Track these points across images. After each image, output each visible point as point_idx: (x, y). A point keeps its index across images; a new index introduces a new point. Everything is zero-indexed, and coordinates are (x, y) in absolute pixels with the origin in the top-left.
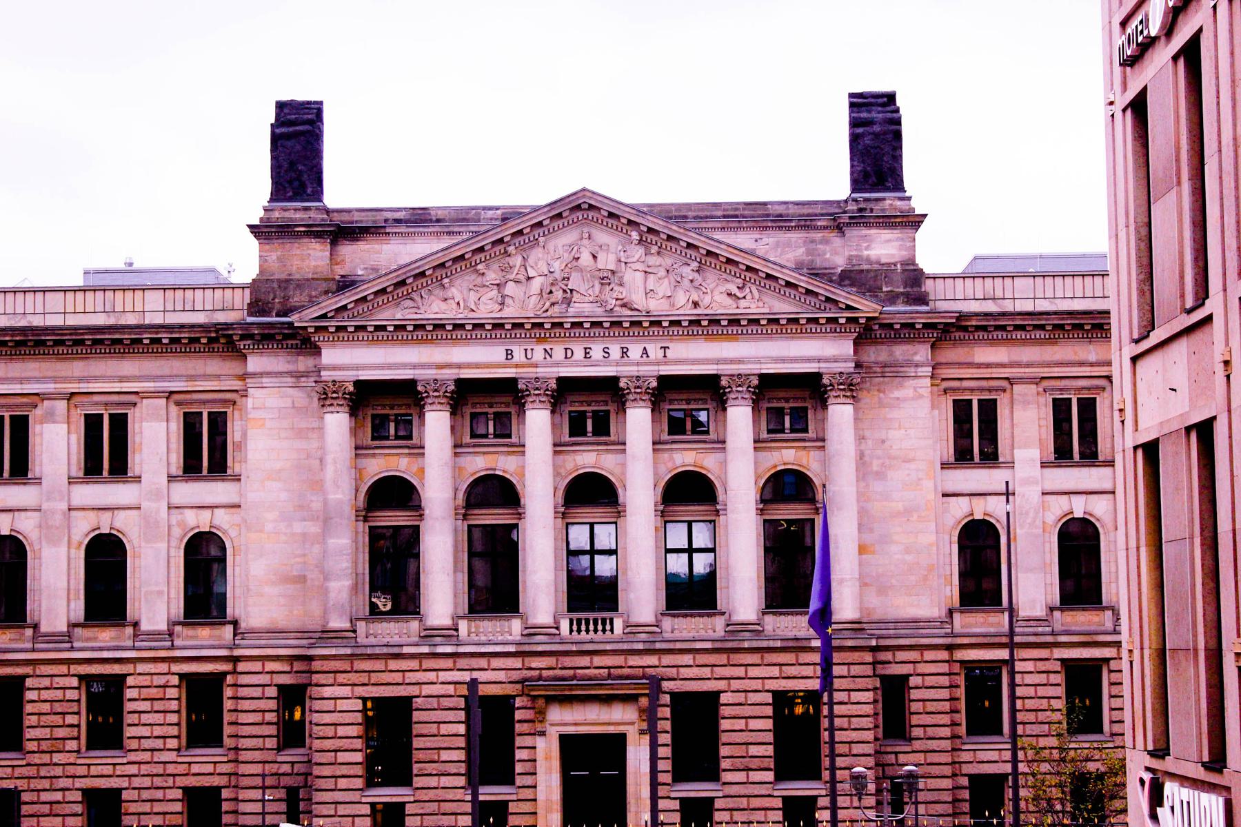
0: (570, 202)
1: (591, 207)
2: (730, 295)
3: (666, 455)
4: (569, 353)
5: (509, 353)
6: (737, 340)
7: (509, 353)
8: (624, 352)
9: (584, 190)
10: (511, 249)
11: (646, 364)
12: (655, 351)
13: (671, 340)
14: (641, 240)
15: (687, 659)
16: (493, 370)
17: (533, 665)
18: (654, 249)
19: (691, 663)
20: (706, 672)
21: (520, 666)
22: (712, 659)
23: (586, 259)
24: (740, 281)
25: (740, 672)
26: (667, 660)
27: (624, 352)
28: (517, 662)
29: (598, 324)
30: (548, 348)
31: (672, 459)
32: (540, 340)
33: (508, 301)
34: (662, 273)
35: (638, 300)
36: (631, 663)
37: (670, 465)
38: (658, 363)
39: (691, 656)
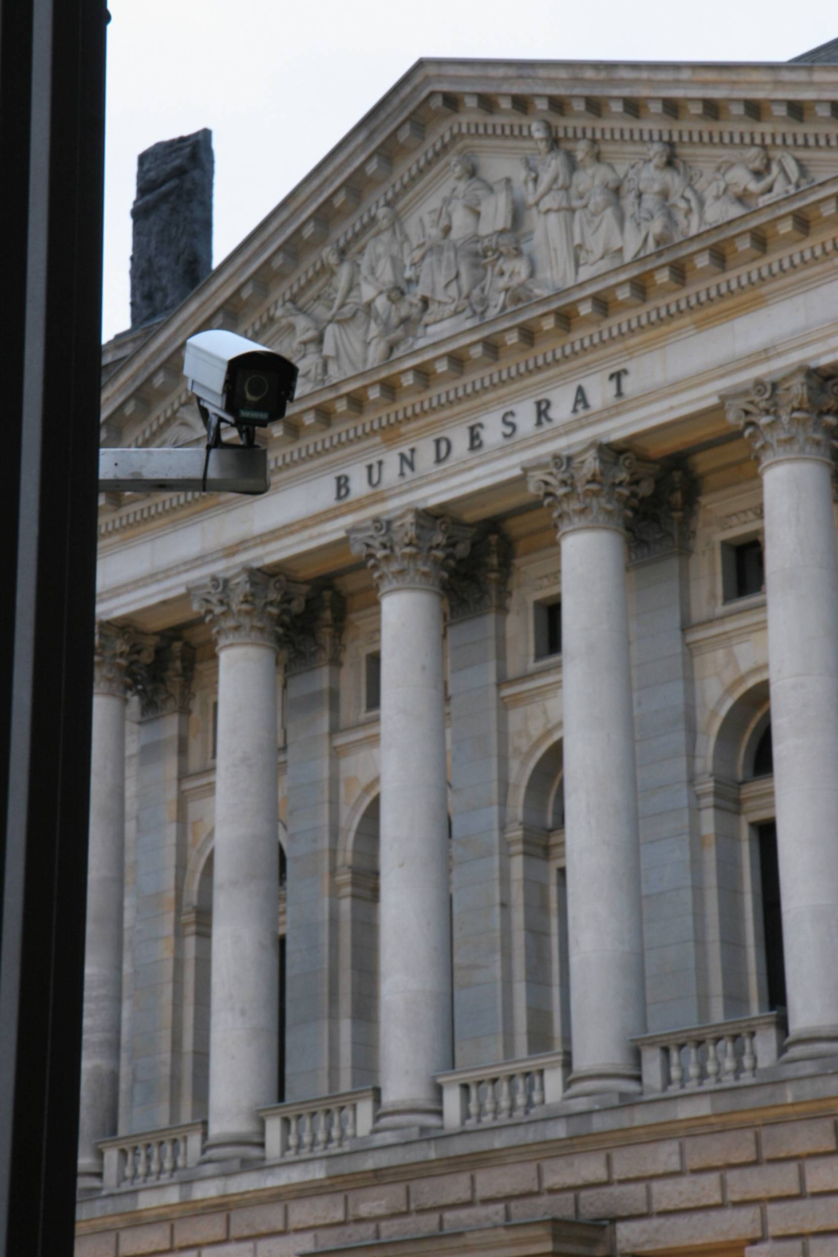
0: (404, 103)
1: (452, 102)
2: (742, 198)
3: (720, 654)
4: (443, 447)
5: (342, 483)
6: (760, 302)
7: (342, 483)
8: (542, 411)
9: (421, 64)
10: (328, 254)
11: (581, 425)
12: (599, 392)
13: (631, 353)
14: (554, 142)
15: (666, 1156)
16: (315, 531)
17: (364, 1210)
18: (581, 150)
19: (674, 1164)
20: (707, 1188)
21: (339, 1216)
22: (715, 1150)
23: (460, 220)
24: (753, 152)
25: (783, 1179)
26: (626, 1163)
27: (542, 411)
28: (328, 1210)
29: (458, 361)
30: (406, 450)
31: (732, 659)
32: (390, 433)
33: (332, 368)
34: (598, 198)
35: (556, 273)
36: (551, 1180)
37: (729, 676)
38: (610, 412)
39: (672, 1147)
